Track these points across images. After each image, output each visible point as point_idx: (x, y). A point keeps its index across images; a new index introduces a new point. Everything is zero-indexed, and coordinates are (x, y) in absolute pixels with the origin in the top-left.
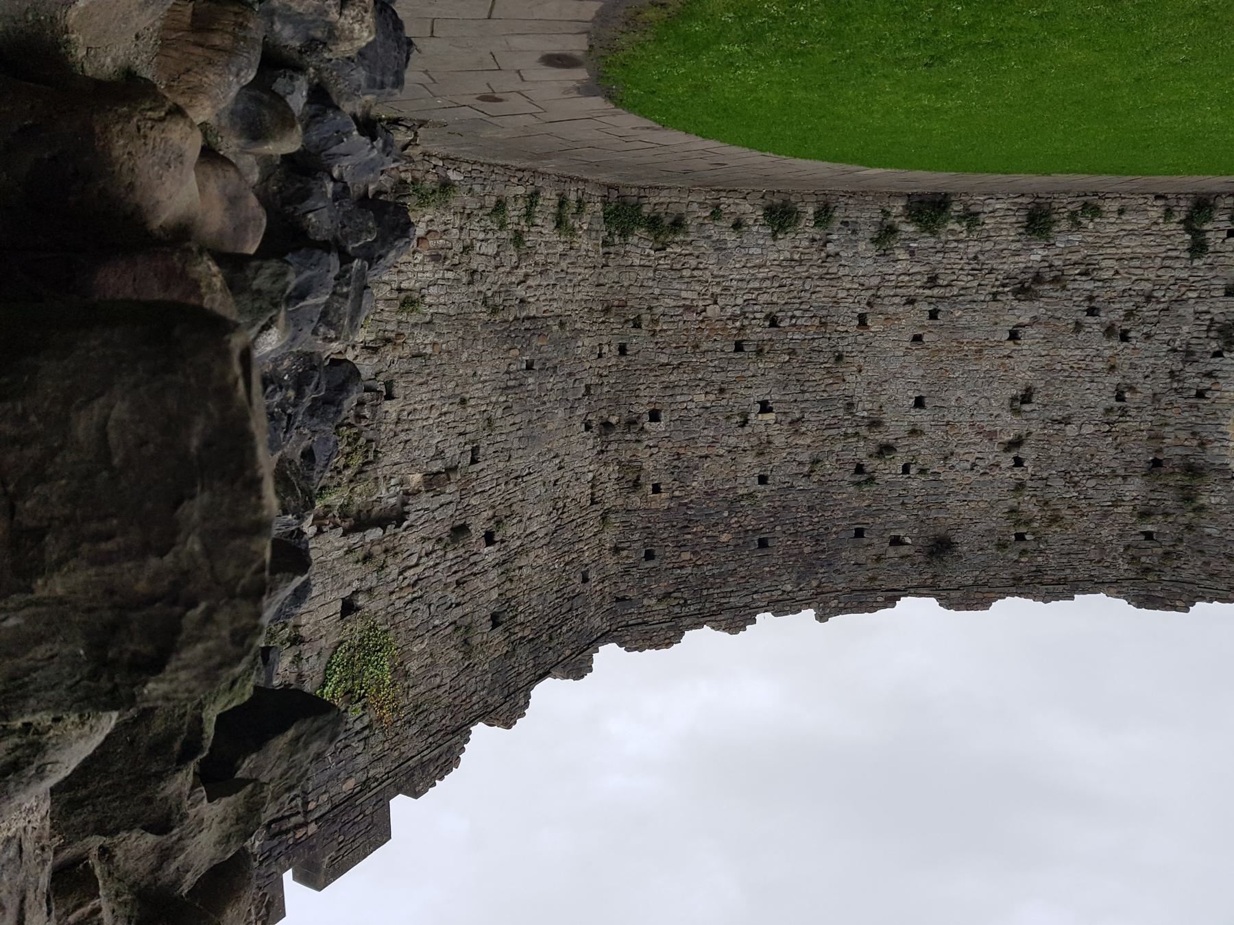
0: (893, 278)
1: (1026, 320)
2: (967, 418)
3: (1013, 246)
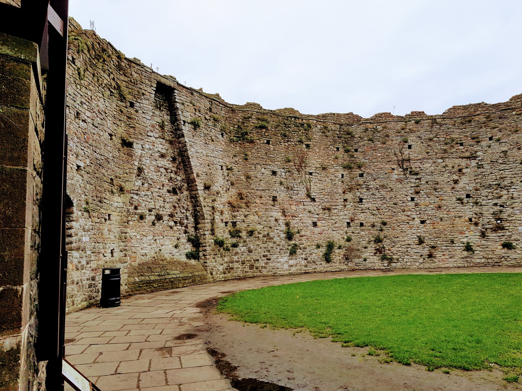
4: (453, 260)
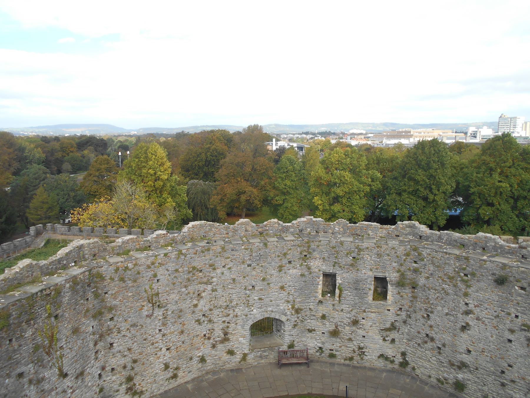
0: (521, 393)
1: (464, 355)
2: (488, 329)
3: (469, 382)
4: (191, 374)
